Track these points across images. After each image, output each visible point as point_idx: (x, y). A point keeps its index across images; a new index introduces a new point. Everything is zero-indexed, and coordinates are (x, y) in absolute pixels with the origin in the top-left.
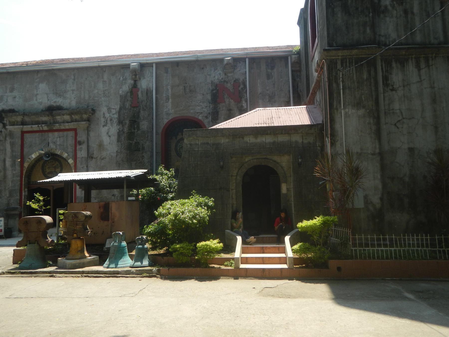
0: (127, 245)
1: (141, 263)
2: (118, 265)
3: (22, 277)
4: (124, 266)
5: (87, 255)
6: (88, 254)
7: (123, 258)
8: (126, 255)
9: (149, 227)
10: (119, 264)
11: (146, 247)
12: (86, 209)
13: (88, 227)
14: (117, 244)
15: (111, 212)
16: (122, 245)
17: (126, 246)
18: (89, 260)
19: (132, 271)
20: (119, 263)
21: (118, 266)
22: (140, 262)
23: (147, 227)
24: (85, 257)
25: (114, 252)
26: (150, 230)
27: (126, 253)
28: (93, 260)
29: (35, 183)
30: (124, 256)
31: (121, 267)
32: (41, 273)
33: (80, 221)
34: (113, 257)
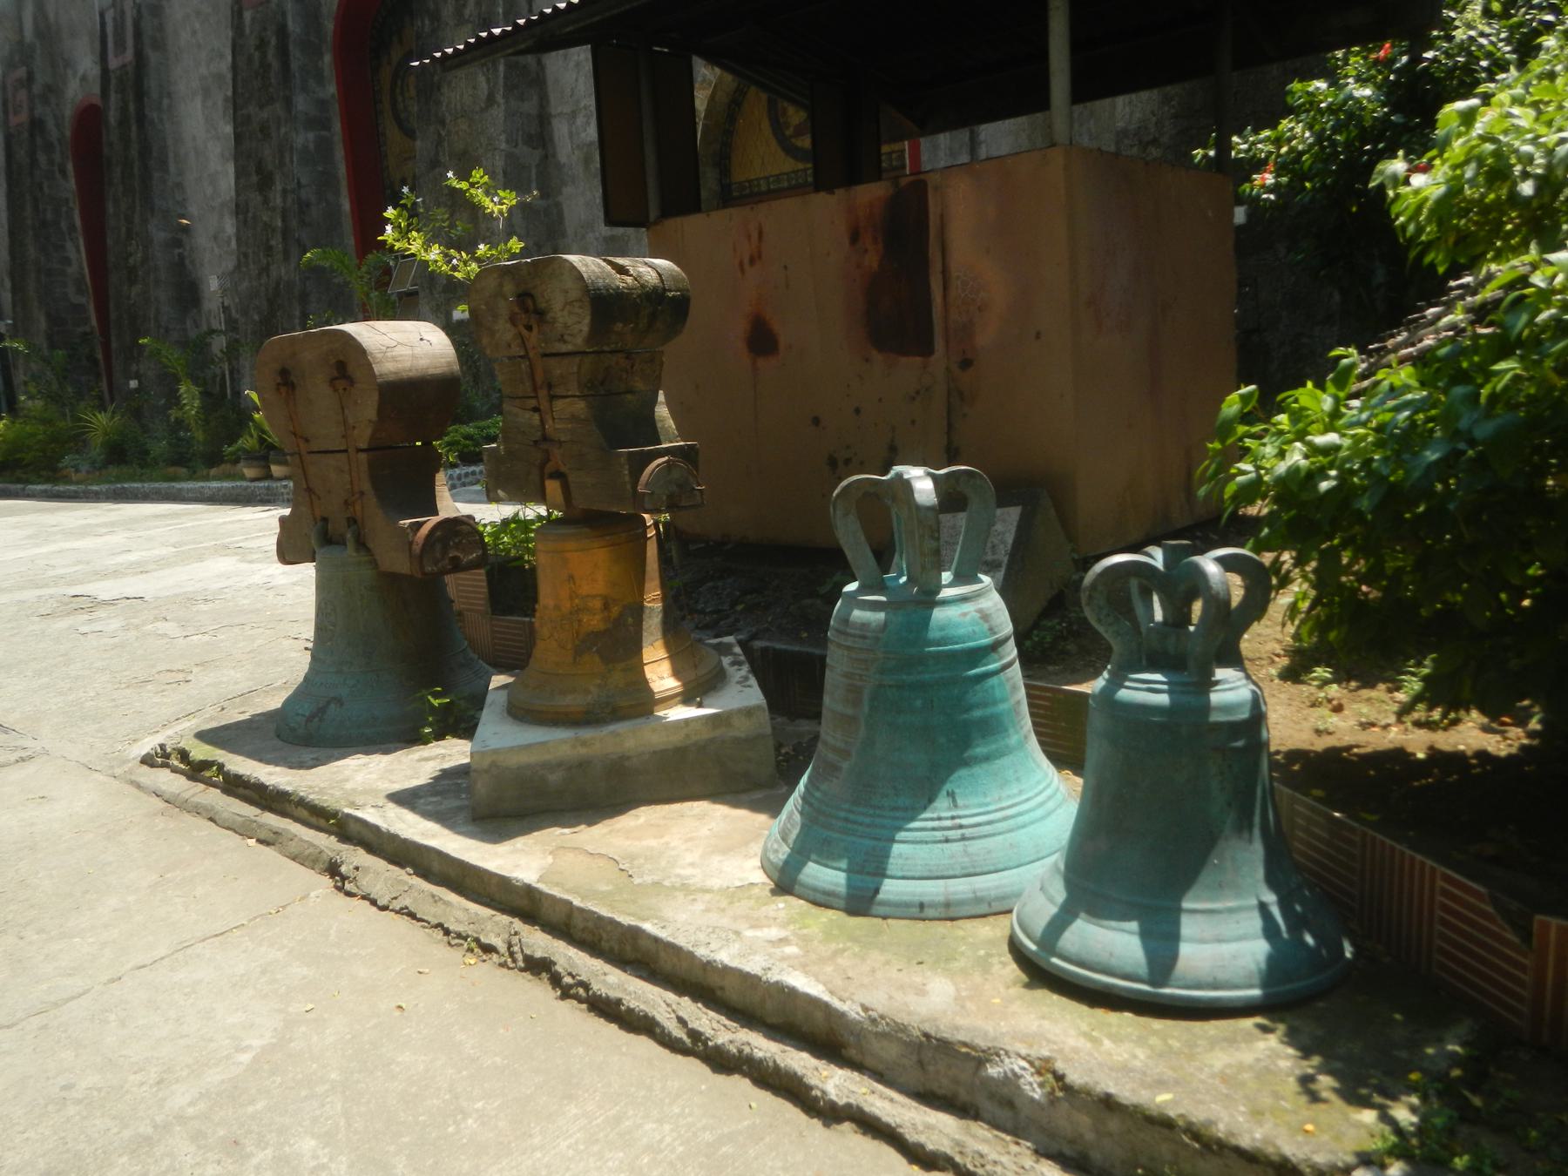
0: (1007, 627)
1: (1145, 935)
2: (881, 873)
3: (211, 819)
4: (961, 903)
5: (661, 677)
6: (676, 673)
7: (951, 795)
8: (987, 758)
9: (1296, 417)
10: (893, 865)
11: (1227, 708)
12: (760, 257)
13: (662, 411)
14: (881, 616)
15: (945, 271)
16: (933, 634)
17: (995, 647)
18: (676, 739)
19: (993, 1071)
20: (897, 849)
21: (891, 889)
22: (1134, 925)
23: (1265, 408)
24: (642, 703)
25: (849, 711)
26: (1296, 456)
27: (991, 727)
28: (712, 740)
29: (748, 191)
30: (966, 763)
31: (922, 906)
32: (304, 813)
33: (564, 348)
34: (845, 765)
